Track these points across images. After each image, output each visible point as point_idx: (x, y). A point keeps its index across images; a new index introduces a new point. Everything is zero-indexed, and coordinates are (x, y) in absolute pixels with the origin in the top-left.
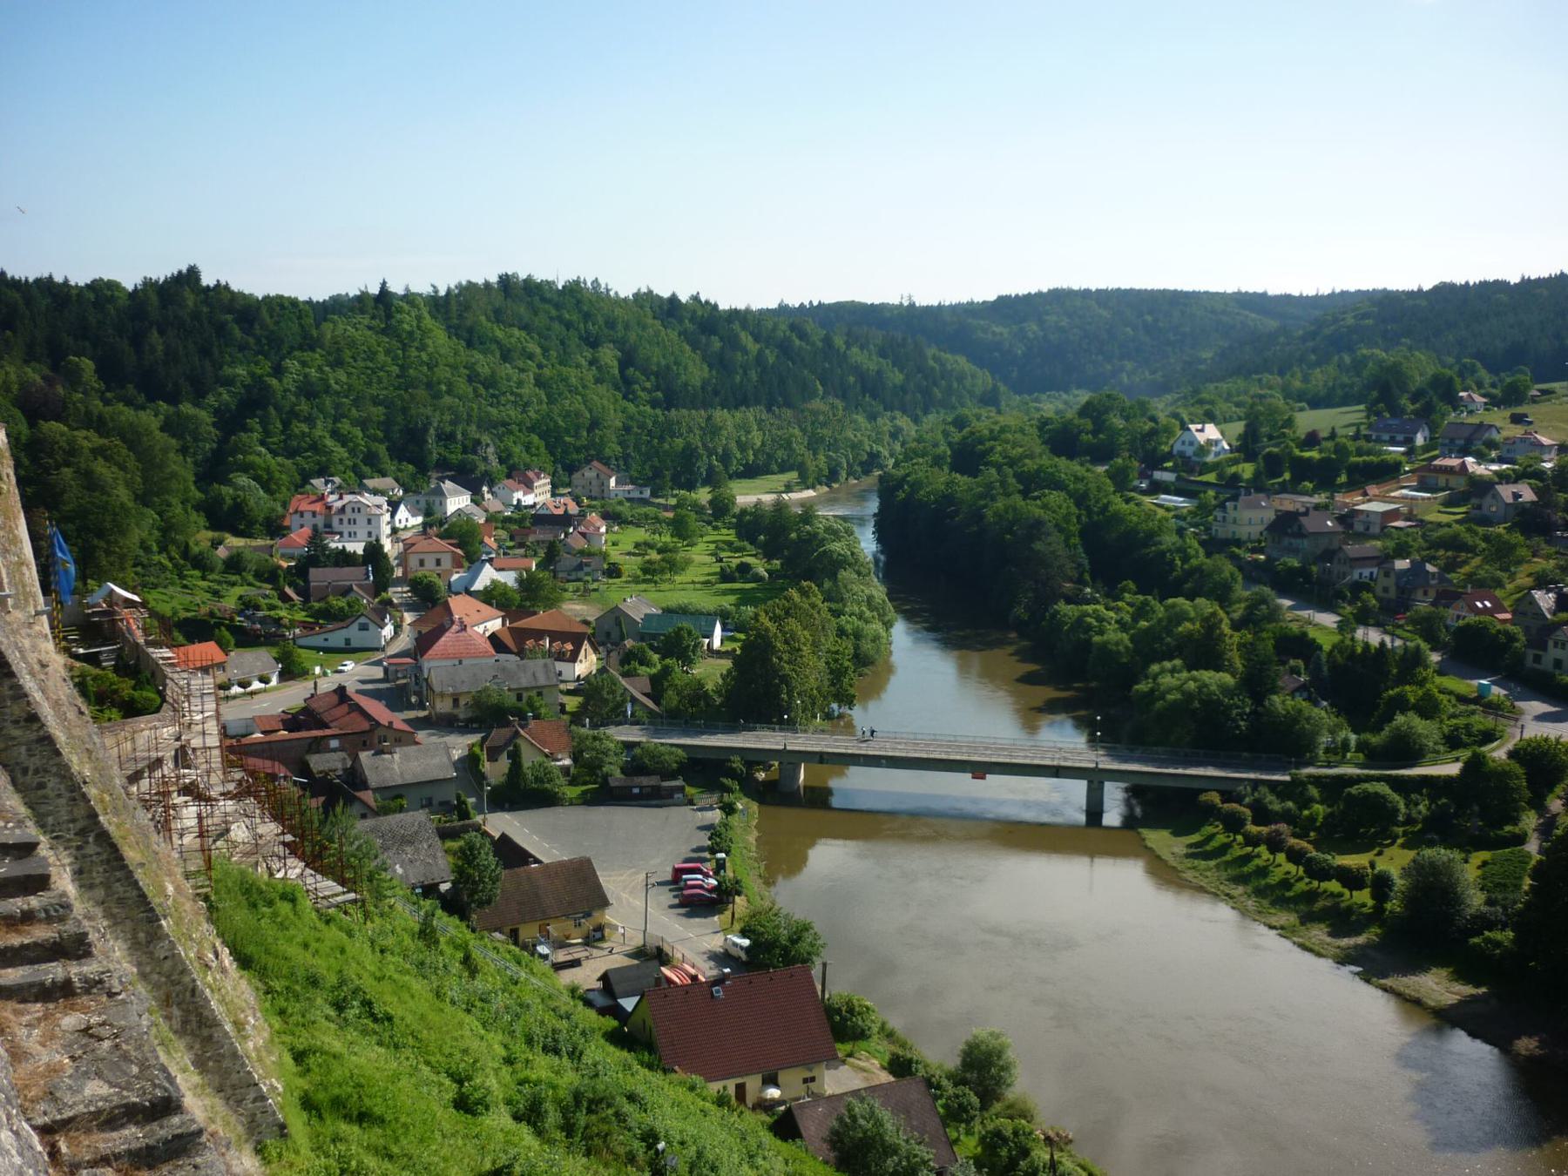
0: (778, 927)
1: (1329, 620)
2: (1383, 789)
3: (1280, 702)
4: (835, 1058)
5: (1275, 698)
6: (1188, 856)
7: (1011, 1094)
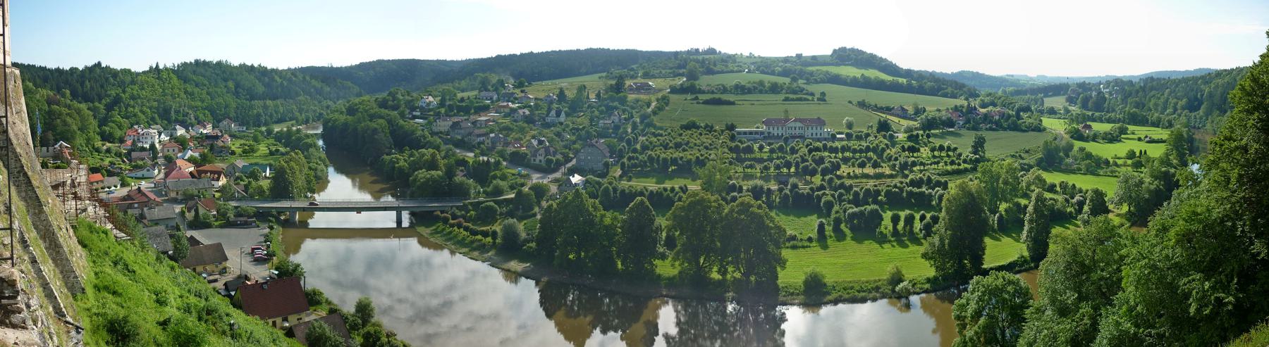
1: (472, 155)
3: (459, 178)
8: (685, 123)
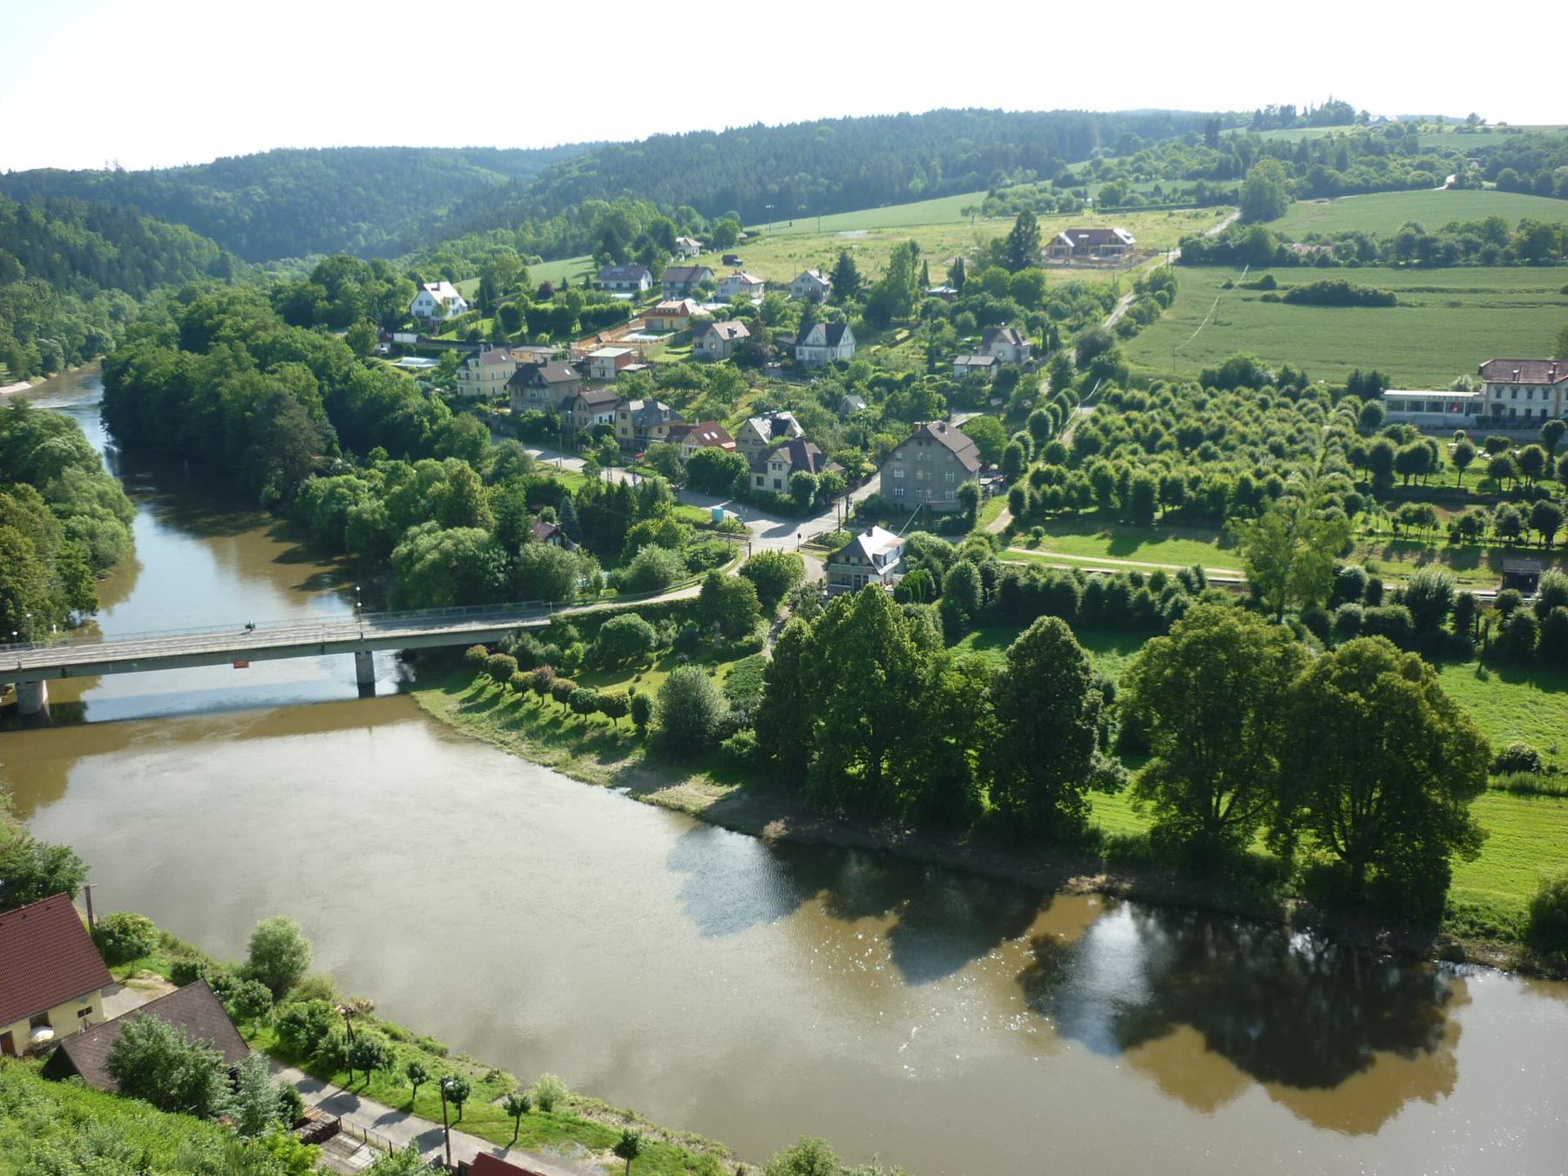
0: (31, 859)
1: (575, 465)
2: (635, 619)
3: (534, 550)
4: (110, 982)
5: (528, 546)
6: (462, 711)
7: (306, 978)
8: (1215, 366)
